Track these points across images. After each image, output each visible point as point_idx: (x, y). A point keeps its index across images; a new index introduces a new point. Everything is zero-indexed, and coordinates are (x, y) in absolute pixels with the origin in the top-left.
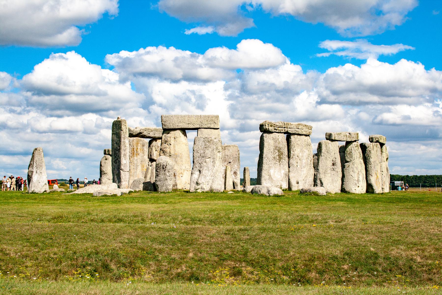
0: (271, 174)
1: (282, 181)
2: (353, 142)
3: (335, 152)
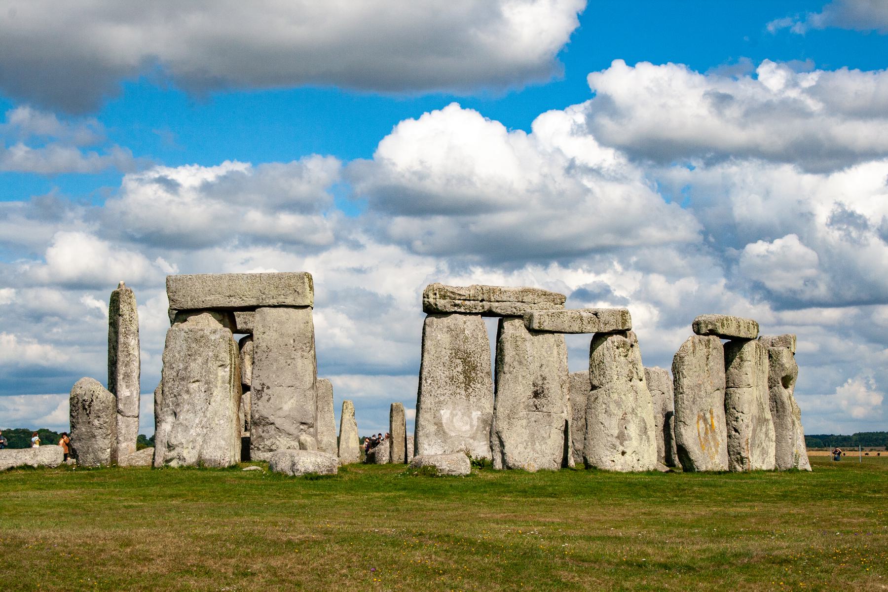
0: (444, 421)
1: (473, 438)
2: (611, 334)
3: (544, 362)
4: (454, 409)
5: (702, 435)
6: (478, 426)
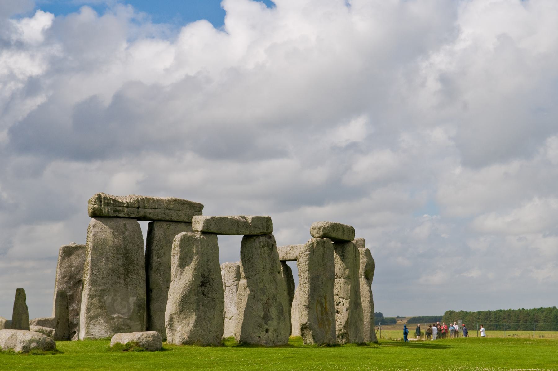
0: (107, 305)
2: (258, 236)
4: (115, 295)
5: (319, 316)
6: (134, 310)
